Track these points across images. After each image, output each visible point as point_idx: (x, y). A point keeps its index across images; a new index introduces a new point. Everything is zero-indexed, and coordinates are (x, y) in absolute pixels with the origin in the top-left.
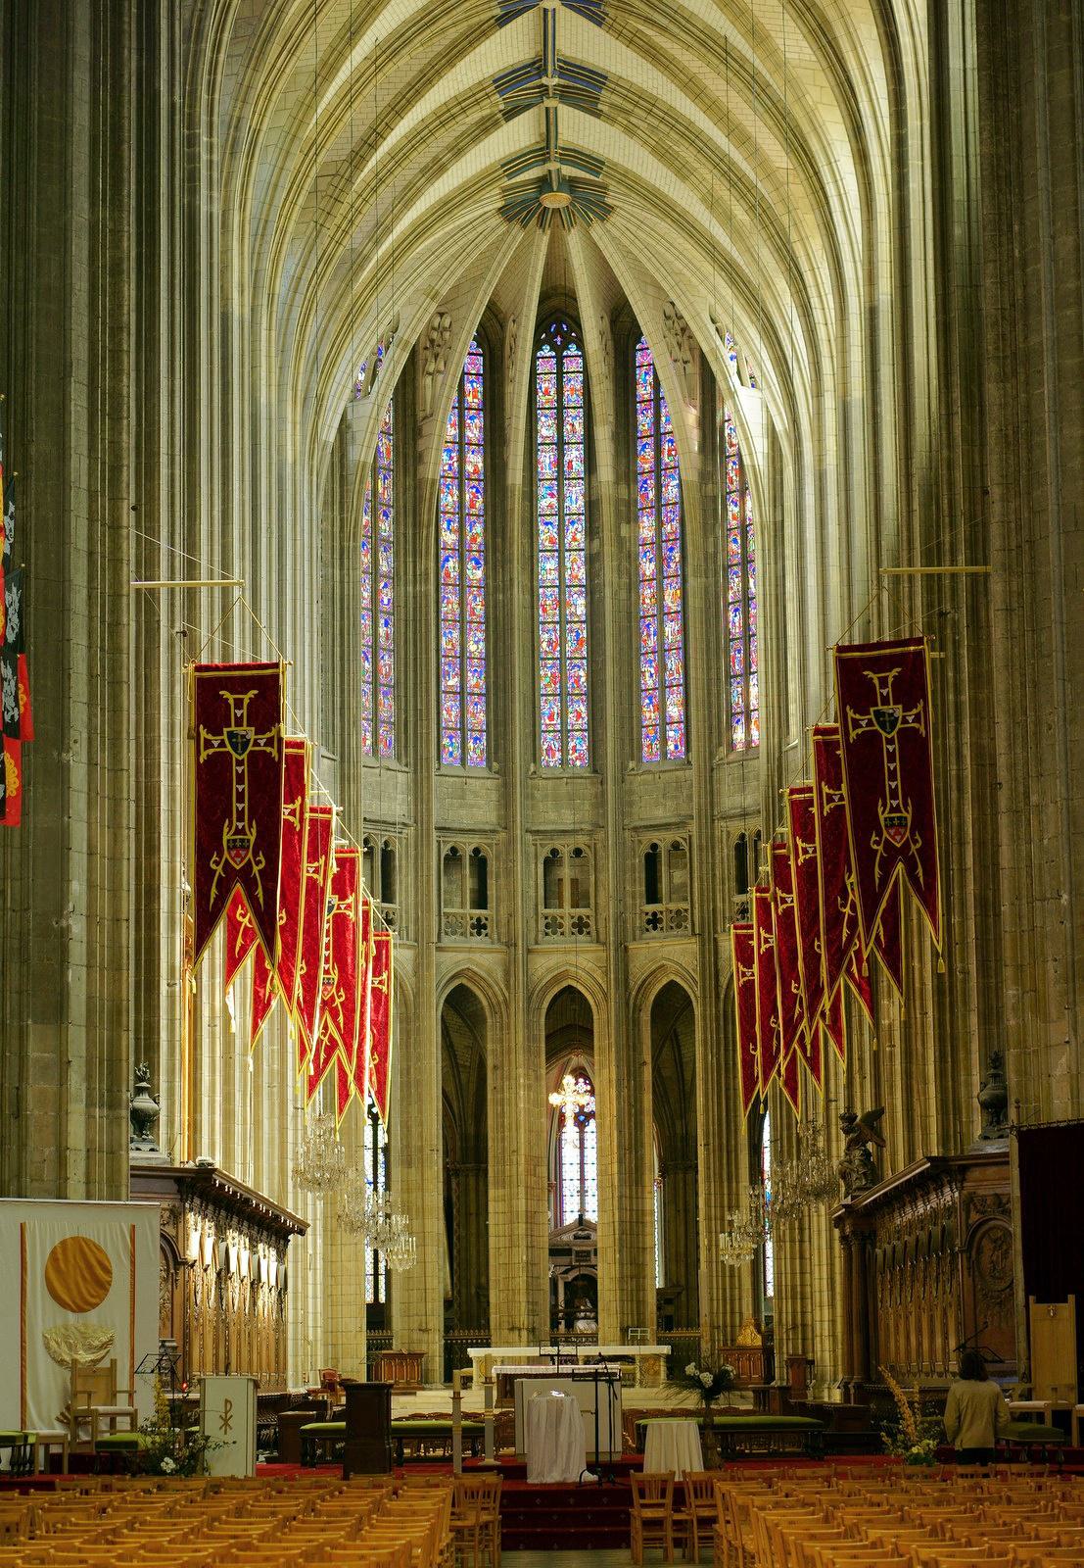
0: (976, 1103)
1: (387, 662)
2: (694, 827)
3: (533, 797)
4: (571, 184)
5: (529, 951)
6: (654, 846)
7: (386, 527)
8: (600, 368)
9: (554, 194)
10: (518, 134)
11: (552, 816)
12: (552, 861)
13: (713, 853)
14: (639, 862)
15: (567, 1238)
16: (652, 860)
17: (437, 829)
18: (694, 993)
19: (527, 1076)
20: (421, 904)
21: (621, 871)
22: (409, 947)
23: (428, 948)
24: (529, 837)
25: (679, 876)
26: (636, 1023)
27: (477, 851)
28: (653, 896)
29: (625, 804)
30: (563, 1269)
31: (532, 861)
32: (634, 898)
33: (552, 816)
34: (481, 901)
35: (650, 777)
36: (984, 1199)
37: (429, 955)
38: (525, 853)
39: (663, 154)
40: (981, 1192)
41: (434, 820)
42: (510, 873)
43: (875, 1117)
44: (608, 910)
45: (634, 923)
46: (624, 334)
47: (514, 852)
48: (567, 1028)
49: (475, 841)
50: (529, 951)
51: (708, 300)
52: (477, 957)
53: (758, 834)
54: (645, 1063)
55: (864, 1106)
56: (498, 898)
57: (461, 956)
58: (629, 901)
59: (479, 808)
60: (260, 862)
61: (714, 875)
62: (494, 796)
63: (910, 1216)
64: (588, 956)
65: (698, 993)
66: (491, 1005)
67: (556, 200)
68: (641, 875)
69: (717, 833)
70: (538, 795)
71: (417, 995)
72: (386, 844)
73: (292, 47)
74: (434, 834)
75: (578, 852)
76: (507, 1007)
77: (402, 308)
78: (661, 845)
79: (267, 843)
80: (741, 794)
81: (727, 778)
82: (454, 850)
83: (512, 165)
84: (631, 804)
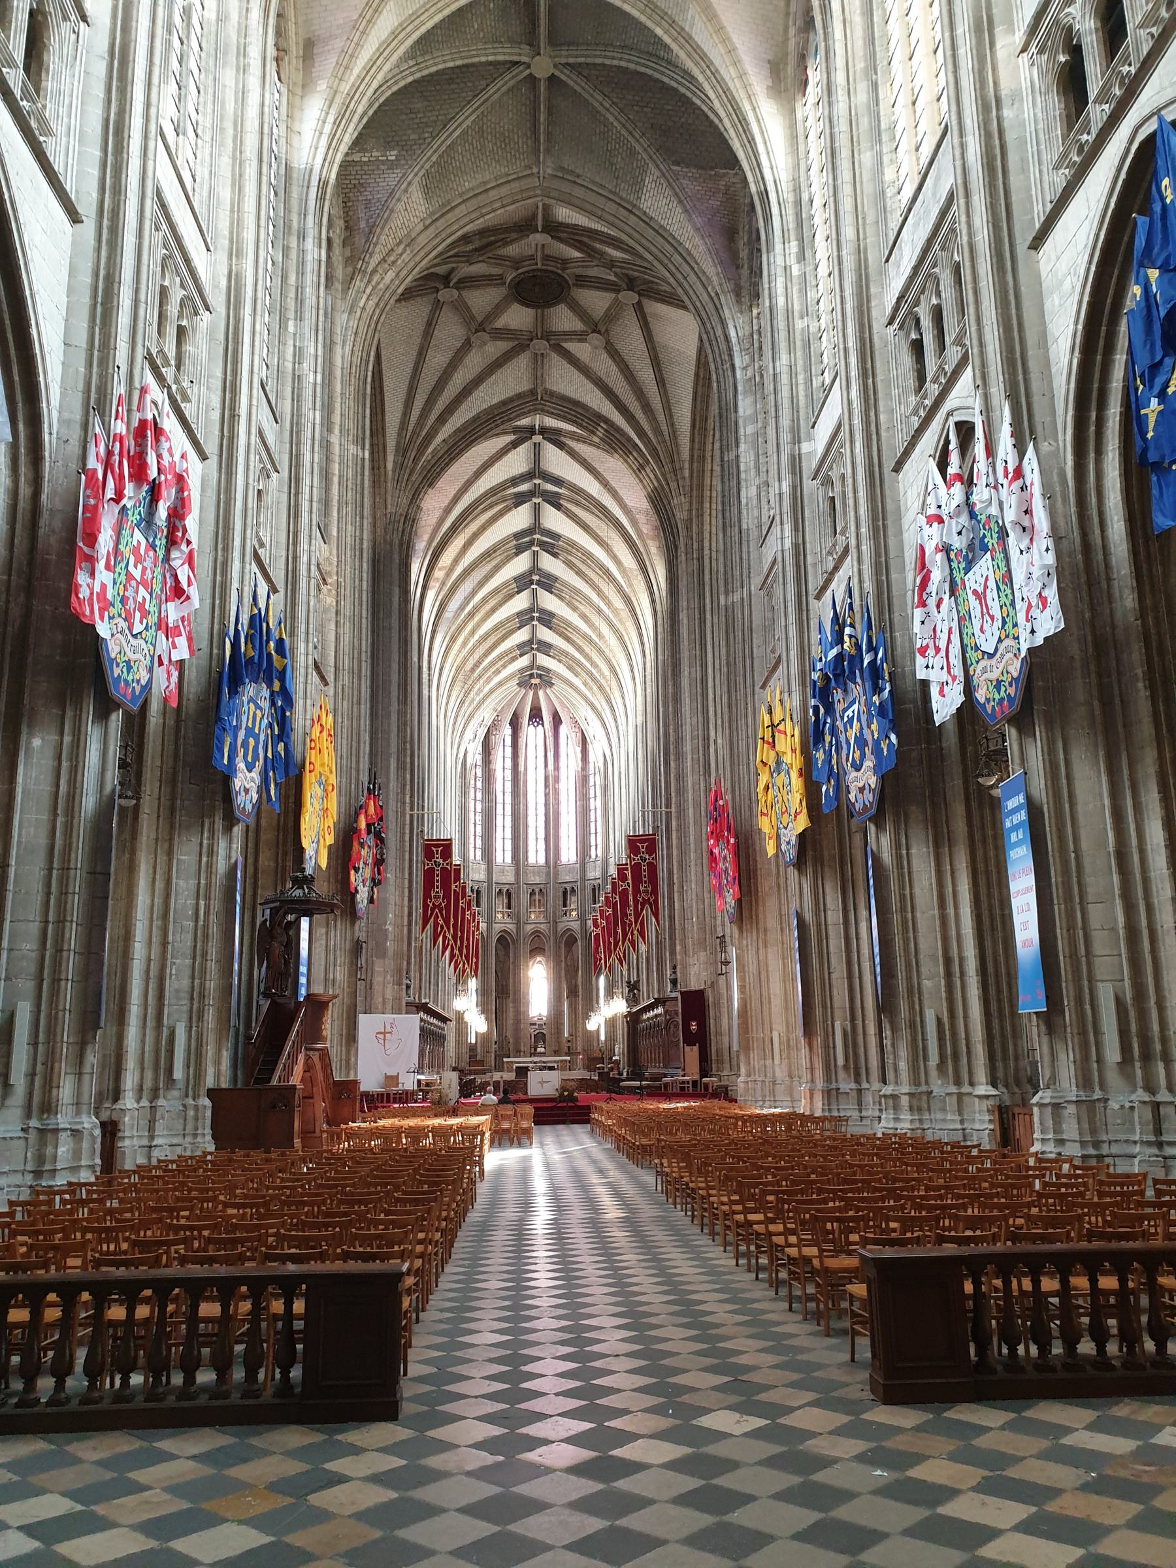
1: (479, 828)
4: (540, 676)
7: (479, 785)
8: (550, 734)
9: (534, 678)
10: (524, 661)
12: (533, 893)
16: (565, 893)
18: (579, 937)
20: (490, 908)
25: (574, 899)
29: (556, 874)
39: (570, 668)
46: (557, 720)
48: (537, 950)
51: (584, 712)
67: (535, 681)
73: (453, 639)
77: (486, 714)
79: (447, 896)
80: (594, 873)
81: (589, 866)
83: (521, 671)
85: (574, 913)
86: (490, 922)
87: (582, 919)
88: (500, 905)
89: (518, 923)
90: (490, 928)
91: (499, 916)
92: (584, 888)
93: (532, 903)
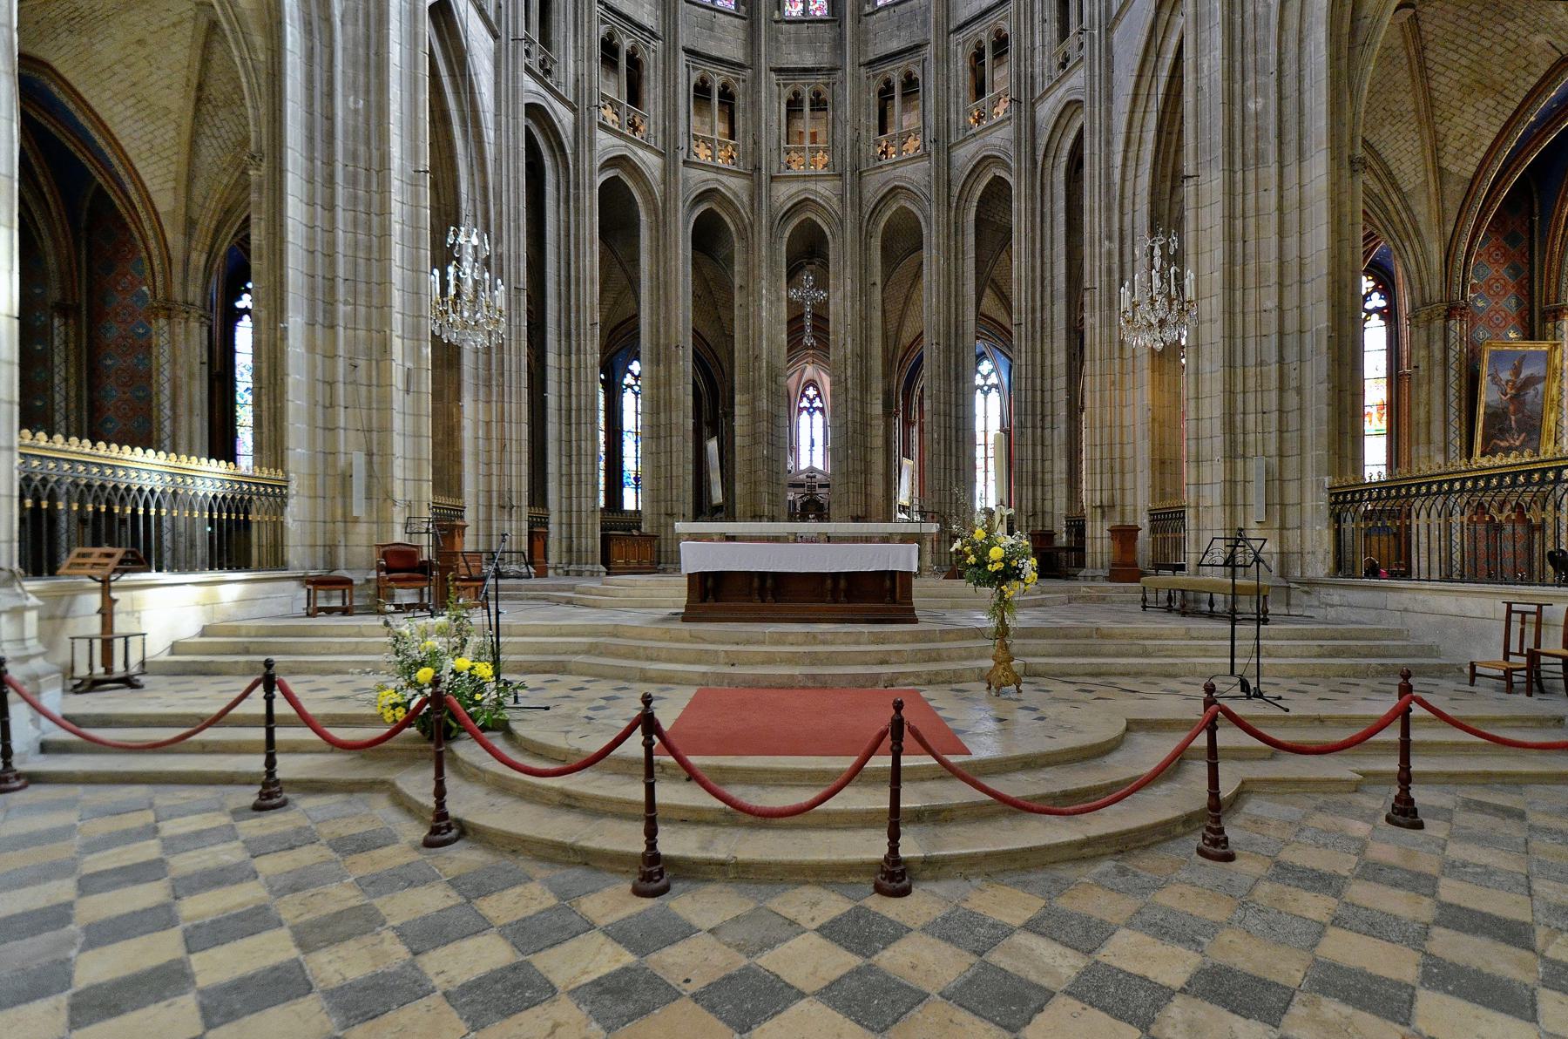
3: (777, 40)
12: (794, 106)
14: (873, 99)
16: (886, 94)
17: (688, 51)
24: (773, 75)
29: (861, 40)
35: (884, 14)
38: (769, 88)
42: (755, 104)
50: (772, 178)
52: (724, 178)
56: (745, 132)
57: (710, 175)
58: (863, 133)
59: (728, 42)
62: (741, 35)
64: (826, 184)
70: (781, 37)
71: (664, 203)
84: (866, 43)
90: (668, 171)
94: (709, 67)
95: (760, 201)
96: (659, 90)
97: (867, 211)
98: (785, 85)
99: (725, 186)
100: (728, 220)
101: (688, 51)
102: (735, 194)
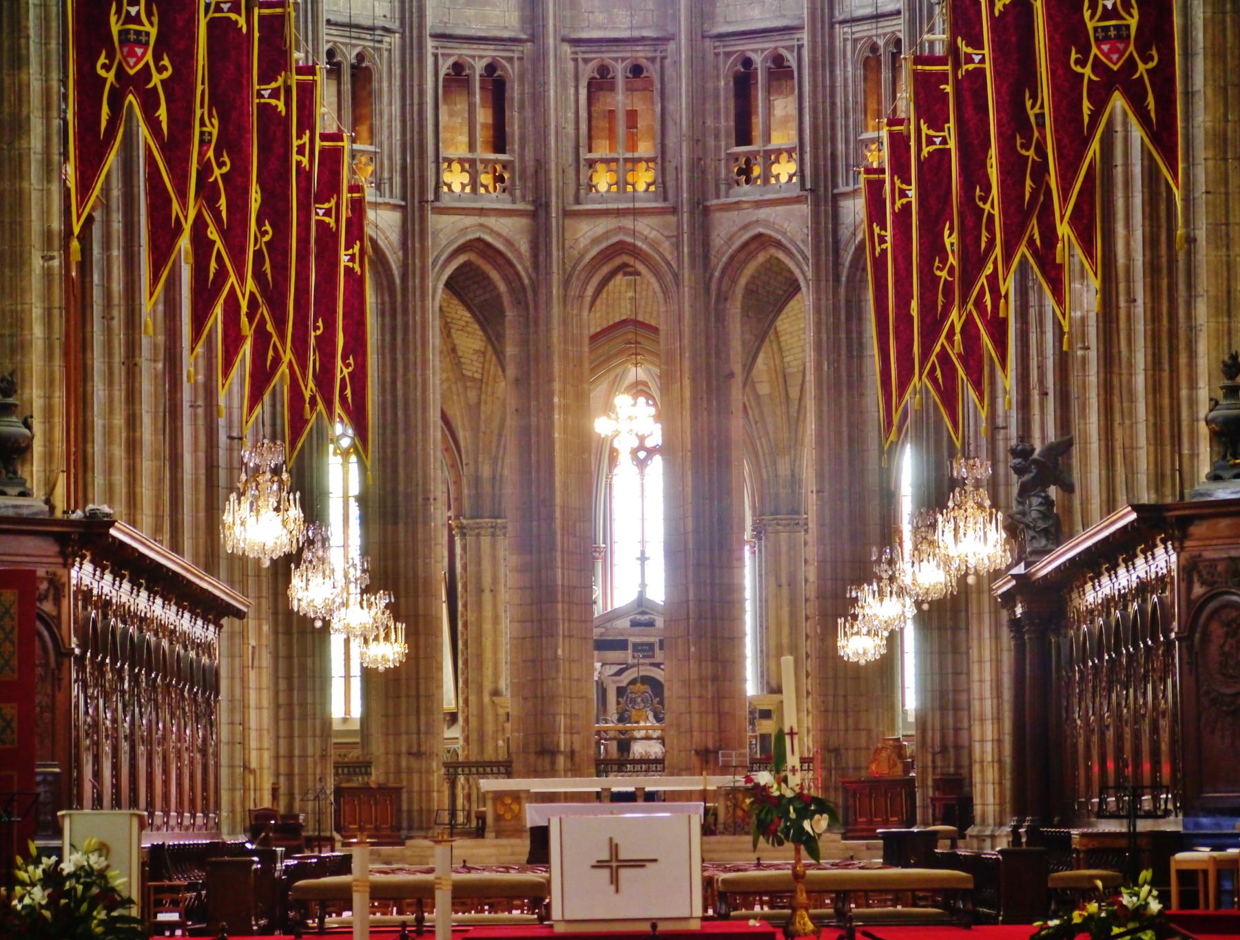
0: (1203, 429)
2: (805, 36)
5: (567, 214)
6: (747, 62)
11: (600, 18)
12: (601, 82)
13: (832, 72)
14: (724, 85)
15: (624, 623)
16: (743, 84)
17: (431, 36)
18: (804, 273)
19: (564, 393)
21: (700, 98)
22: (395, 207)
23: (422, 209)
24: (567, 49)
25: (784, 106)
26: (721, 318)
27: (491, 68)
28: (744, 137)
30: (616, 668)
31: (571, 83)
32: (717, 137)
33: (600, 18)
34: (499, 142)
36: (1213, 563)
37: (423, 219)
38: (561, 73)
40: (1208, 554)
41: (431, 22)
42: (538, 99)
43: (1062, 449)
44: (682, 155)
45: (717, 173)
47: (545, 70)
49: (490, 52)
50: (567, 214)
52: (491, 221)
53: (898, 42)
54: (732, 375)
55: (1044, 433)
56: (523, 138)
57: (469, 221)
58: (711, 142)
60: (165, 68)
61: (833, 104)
63: (1107, 591)
64: (653, 221)
65: (810, 275)
66: (512, 290)
68: (727, 104)
69: (838, 43)
72: (360, 57)
74: (430, 44)
75: (637, 70)
76: (535, 293)
78: (758, 59)
82: (458, 67)
85: (785, 169)
86: (417, 201)
87: (821, 191)
88: (457, 132)
89: (538, 213)
91: (456, 179)
92: (826, 58)
93: (597, 122)
94: (465, 51)
95: (549, 254)
96: (396, 108)
97: (719, 262)
98: (586, 61)
99: (492, 231)
100: (495, 275)
101: (436, 36)
102: (509, 242)
